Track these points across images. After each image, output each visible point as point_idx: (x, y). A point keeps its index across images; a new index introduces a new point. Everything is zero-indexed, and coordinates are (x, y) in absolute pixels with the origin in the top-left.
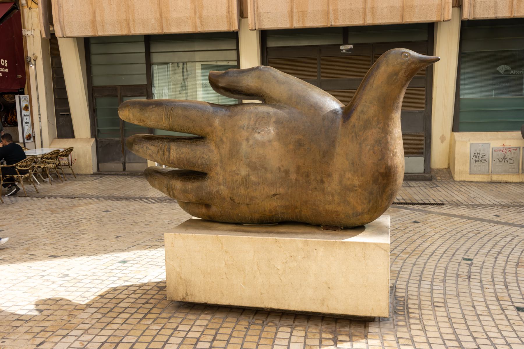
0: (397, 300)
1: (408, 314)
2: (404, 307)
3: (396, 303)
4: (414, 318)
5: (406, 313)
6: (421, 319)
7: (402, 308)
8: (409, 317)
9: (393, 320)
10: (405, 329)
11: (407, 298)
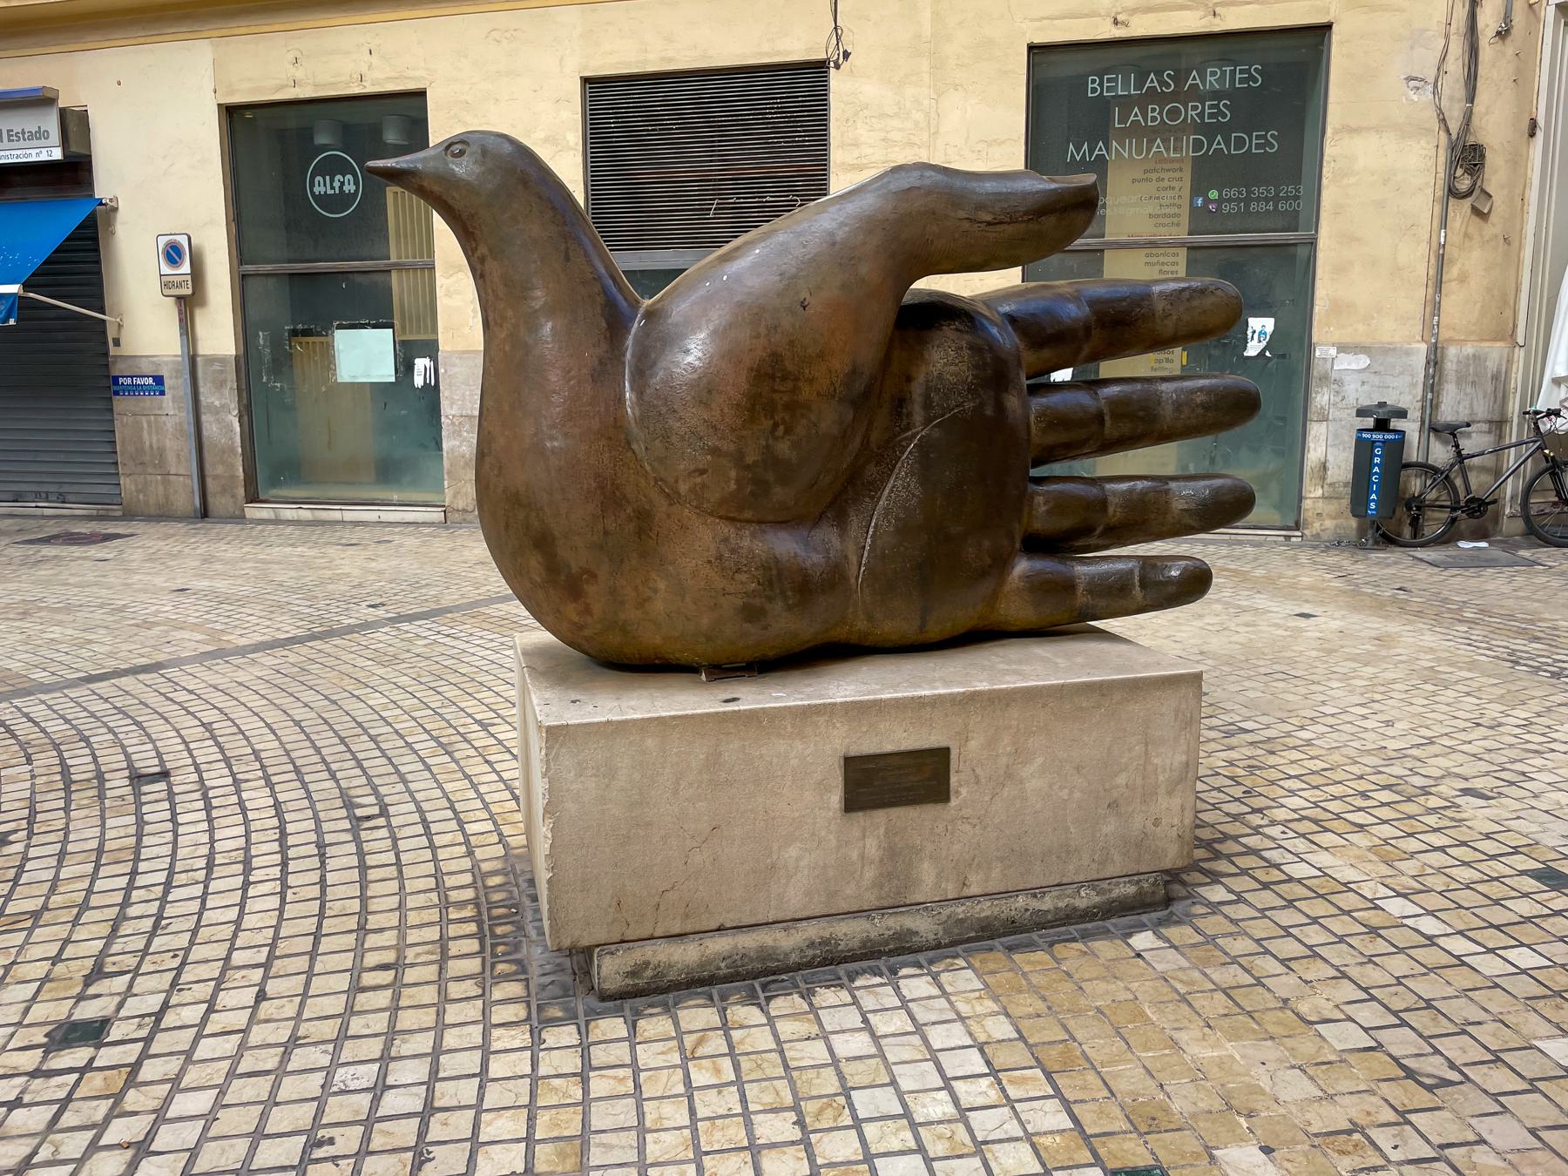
0: (518, 962)
1: (480, 913)
2: (493, 935)
3: (517, 947)
4: (461, 904)
5: (485, 917)
6: (445, 905)
7: (499, 930)
8: (477, 906)
9: (517, 885)
10: (485, 867)
11: (486, 979)
